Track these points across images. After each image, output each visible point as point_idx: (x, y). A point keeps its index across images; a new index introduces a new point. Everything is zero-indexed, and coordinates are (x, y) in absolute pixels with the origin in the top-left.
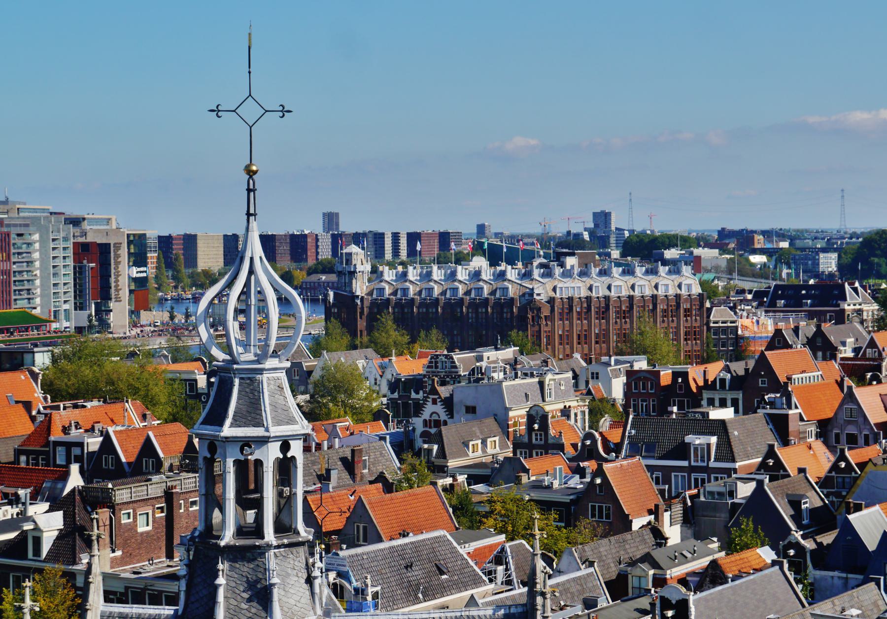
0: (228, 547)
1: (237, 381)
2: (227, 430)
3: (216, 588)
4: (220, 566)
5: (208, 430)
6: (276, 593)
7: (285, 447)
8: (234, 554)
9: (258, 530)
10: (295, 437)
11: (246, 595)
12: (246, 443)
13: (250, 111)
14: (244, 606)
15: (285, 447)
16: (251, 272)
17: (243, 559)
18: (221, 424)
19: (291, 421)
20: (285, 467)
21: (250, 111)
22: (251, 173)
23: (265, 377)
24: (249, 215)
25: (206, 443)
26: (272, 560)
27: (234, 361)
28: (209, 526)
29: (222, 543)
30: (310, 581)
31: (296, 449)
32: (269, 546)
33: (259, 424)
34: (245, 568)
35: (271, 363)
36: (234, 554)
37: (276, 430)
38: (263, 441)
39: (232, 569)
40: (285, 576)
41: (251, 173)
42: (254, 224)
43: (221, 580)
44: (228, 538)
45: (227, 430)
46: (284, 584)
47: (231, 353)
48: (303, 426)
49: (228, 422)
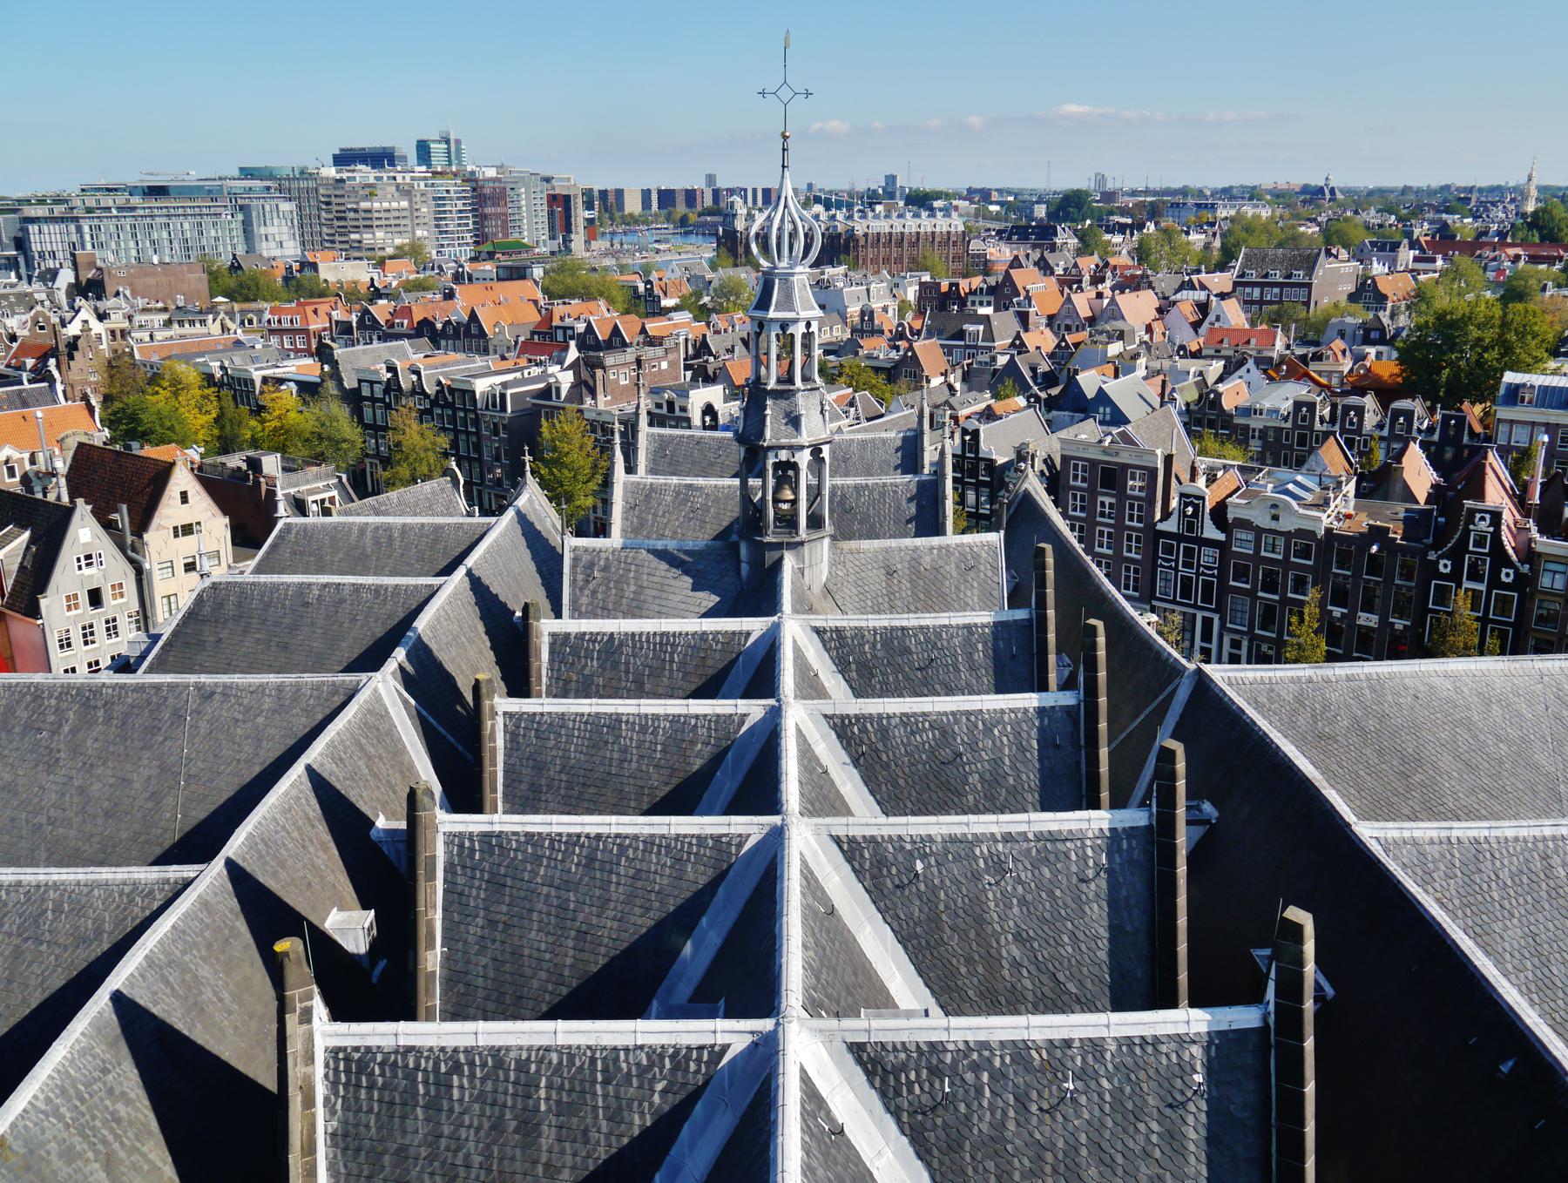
0: (772, 391)
1: (777, 281)
2: (772, 314)
3: (765, 416)
4: (768, 402)
5: (758, 314)
6: (803, 420)
7: (808, 325)
8: (777, 395)
9: (791, 381)
10: (814, 319)
11: (784, 421)
12: (784, 325)
13: (785, 94)
14: (783, 428)
15: (808, 325)
16: (785, 207)
17: (782, 398)
18: (767, 309)
19: (812, 308)
20: (808, 337)
21: (785, 94)
22: (785, 138)
23: (795, 278)
24: (783, 167)
25: (756, 323)
26: (800, 398)
27: (775, 268)
28: (758, 377)
29: (769, 388)
30: (822, 412)
31: (814, 328)
32: (799, 390)
33: (792, 310)
34: (783, 403)
35: (799, 269)
36: (777, 395)
37: (804, 314)
38: (796, 321)
39: (775, 404)
40: (808, 409)
41: (785, 138)
42: (787, 173)
43: (768, 412)
44: (772, 384)
45: (772, 314)
46: (807, 415)
47: (773, 263)
48: (818, 313)
49: (772, 308)
